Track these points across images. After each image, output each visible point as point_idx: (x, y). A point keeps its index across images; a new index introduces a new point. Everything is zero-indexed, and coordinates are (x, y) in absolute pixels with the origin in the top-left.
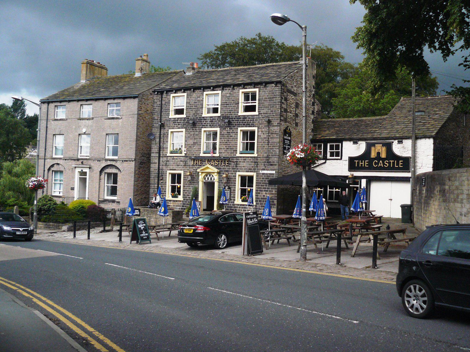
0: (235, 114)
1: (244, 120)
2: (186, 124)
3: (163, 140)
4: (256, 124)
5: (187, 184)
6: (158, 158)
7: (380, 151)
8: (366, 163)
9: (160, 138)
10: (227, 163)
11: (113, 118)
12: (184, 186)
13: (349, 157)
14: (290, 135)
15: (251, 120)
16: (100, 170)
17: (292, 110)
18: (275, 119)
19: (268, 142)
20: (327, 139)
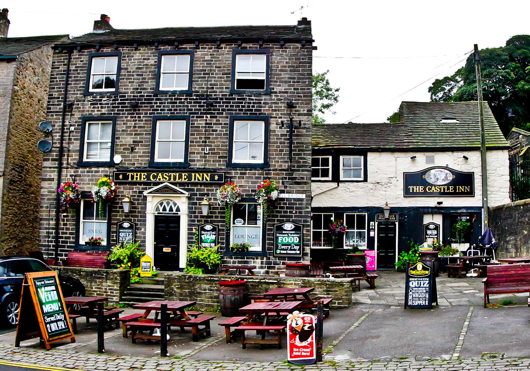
0: (221, 92)
1: (242, 103)
2: (118, 107)
3: (69, 136)
4: (264, 110)
15: (253, 103)
18: (302, 103)
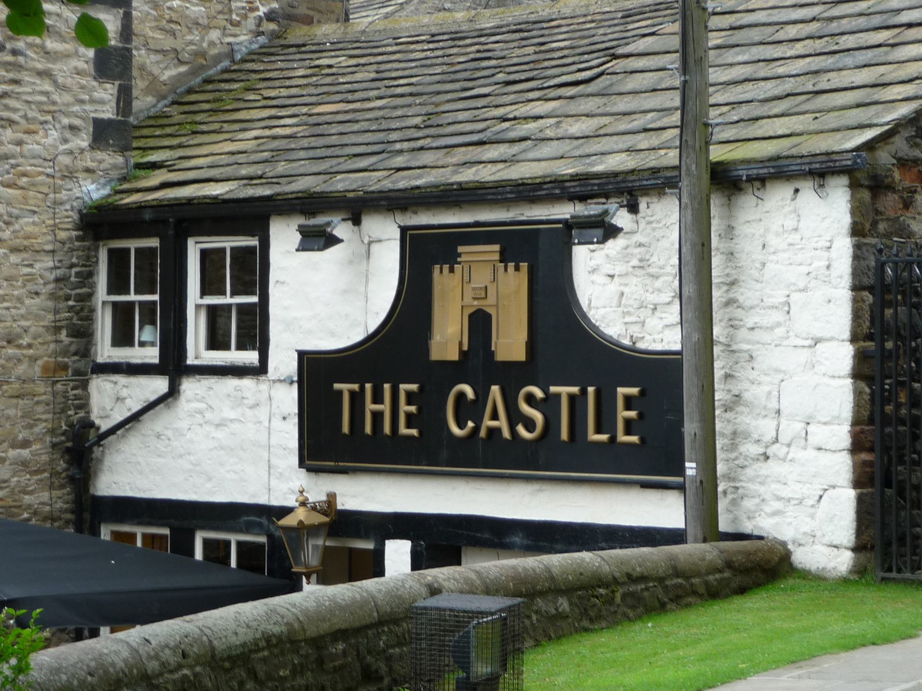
7: (488, 305)
13: (302, 354)
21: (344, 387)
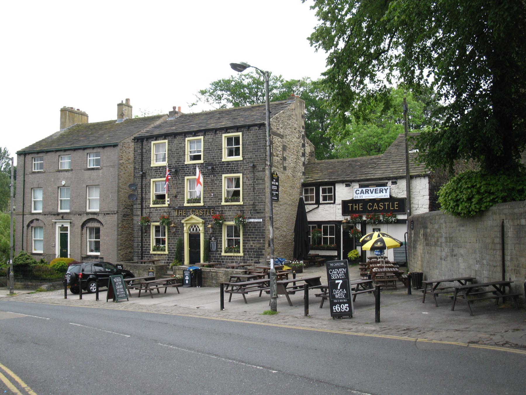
0: (218, 161)
1: (228, 166)
5: (171, 236)
6: (140, 210)
8: (360, 207)
9: (142, 188)
10: (212, 213)
11: (93, 169)
12: (168, 239)
14: (277, 180)
15: (235, 166)
16: (81, 224)
17: (278, 153)
18: (260, 164)
19: (254, 189)
20: (319, 182)
21: (350, 205)
